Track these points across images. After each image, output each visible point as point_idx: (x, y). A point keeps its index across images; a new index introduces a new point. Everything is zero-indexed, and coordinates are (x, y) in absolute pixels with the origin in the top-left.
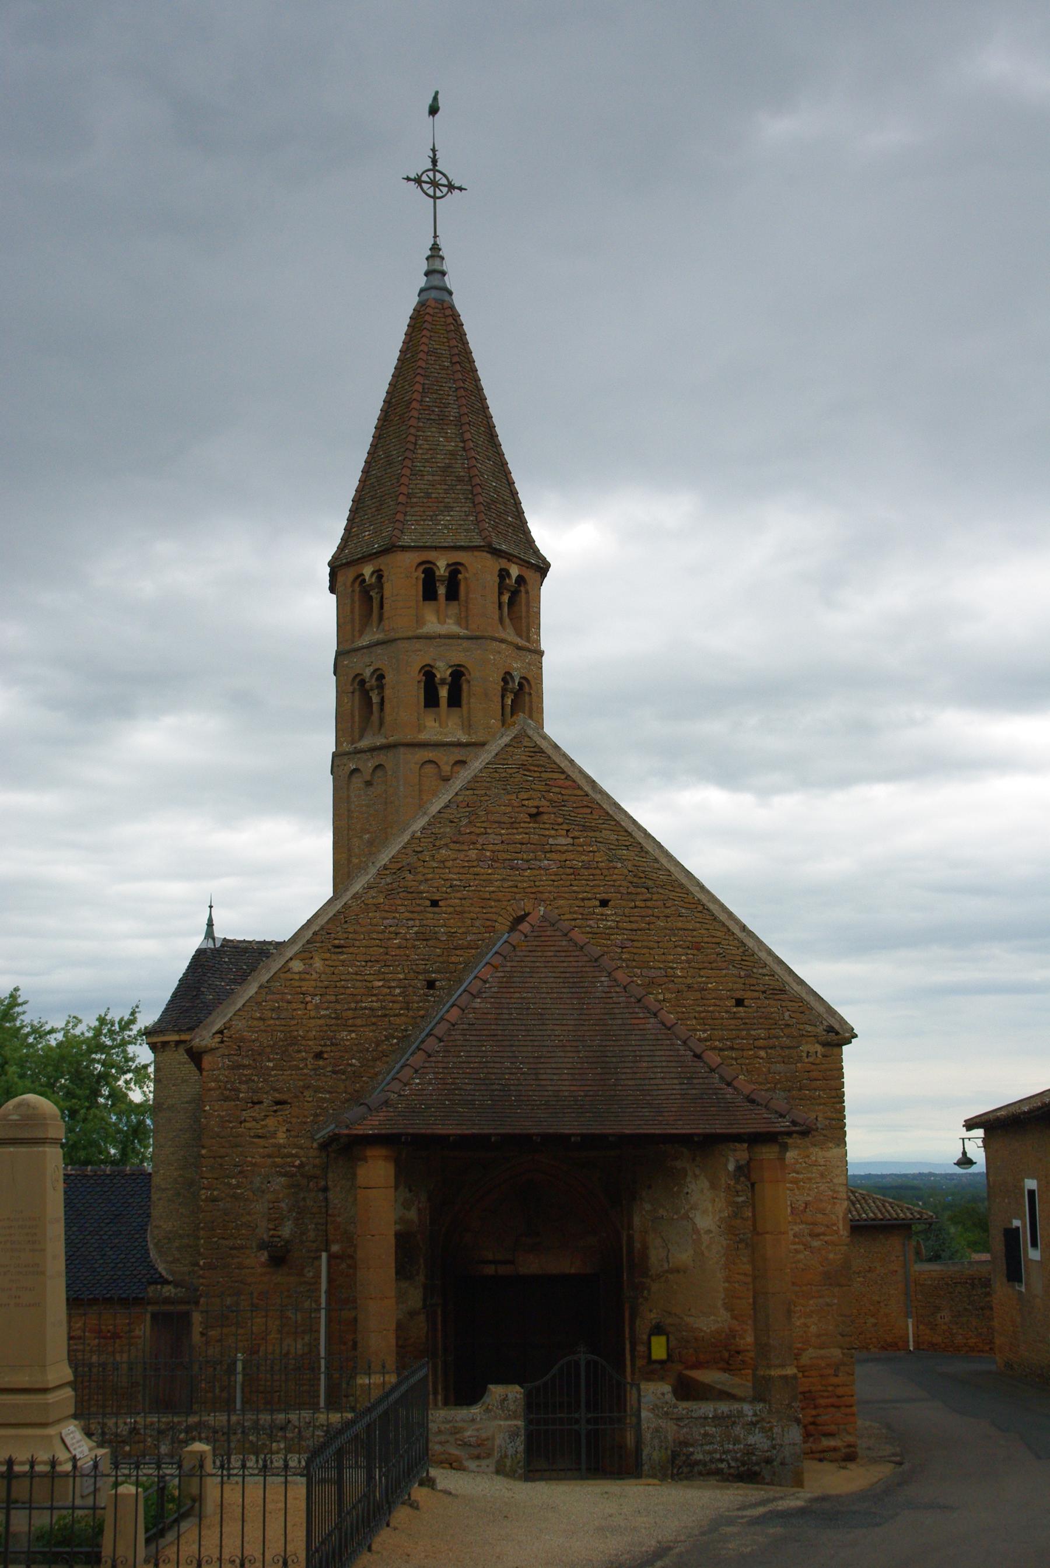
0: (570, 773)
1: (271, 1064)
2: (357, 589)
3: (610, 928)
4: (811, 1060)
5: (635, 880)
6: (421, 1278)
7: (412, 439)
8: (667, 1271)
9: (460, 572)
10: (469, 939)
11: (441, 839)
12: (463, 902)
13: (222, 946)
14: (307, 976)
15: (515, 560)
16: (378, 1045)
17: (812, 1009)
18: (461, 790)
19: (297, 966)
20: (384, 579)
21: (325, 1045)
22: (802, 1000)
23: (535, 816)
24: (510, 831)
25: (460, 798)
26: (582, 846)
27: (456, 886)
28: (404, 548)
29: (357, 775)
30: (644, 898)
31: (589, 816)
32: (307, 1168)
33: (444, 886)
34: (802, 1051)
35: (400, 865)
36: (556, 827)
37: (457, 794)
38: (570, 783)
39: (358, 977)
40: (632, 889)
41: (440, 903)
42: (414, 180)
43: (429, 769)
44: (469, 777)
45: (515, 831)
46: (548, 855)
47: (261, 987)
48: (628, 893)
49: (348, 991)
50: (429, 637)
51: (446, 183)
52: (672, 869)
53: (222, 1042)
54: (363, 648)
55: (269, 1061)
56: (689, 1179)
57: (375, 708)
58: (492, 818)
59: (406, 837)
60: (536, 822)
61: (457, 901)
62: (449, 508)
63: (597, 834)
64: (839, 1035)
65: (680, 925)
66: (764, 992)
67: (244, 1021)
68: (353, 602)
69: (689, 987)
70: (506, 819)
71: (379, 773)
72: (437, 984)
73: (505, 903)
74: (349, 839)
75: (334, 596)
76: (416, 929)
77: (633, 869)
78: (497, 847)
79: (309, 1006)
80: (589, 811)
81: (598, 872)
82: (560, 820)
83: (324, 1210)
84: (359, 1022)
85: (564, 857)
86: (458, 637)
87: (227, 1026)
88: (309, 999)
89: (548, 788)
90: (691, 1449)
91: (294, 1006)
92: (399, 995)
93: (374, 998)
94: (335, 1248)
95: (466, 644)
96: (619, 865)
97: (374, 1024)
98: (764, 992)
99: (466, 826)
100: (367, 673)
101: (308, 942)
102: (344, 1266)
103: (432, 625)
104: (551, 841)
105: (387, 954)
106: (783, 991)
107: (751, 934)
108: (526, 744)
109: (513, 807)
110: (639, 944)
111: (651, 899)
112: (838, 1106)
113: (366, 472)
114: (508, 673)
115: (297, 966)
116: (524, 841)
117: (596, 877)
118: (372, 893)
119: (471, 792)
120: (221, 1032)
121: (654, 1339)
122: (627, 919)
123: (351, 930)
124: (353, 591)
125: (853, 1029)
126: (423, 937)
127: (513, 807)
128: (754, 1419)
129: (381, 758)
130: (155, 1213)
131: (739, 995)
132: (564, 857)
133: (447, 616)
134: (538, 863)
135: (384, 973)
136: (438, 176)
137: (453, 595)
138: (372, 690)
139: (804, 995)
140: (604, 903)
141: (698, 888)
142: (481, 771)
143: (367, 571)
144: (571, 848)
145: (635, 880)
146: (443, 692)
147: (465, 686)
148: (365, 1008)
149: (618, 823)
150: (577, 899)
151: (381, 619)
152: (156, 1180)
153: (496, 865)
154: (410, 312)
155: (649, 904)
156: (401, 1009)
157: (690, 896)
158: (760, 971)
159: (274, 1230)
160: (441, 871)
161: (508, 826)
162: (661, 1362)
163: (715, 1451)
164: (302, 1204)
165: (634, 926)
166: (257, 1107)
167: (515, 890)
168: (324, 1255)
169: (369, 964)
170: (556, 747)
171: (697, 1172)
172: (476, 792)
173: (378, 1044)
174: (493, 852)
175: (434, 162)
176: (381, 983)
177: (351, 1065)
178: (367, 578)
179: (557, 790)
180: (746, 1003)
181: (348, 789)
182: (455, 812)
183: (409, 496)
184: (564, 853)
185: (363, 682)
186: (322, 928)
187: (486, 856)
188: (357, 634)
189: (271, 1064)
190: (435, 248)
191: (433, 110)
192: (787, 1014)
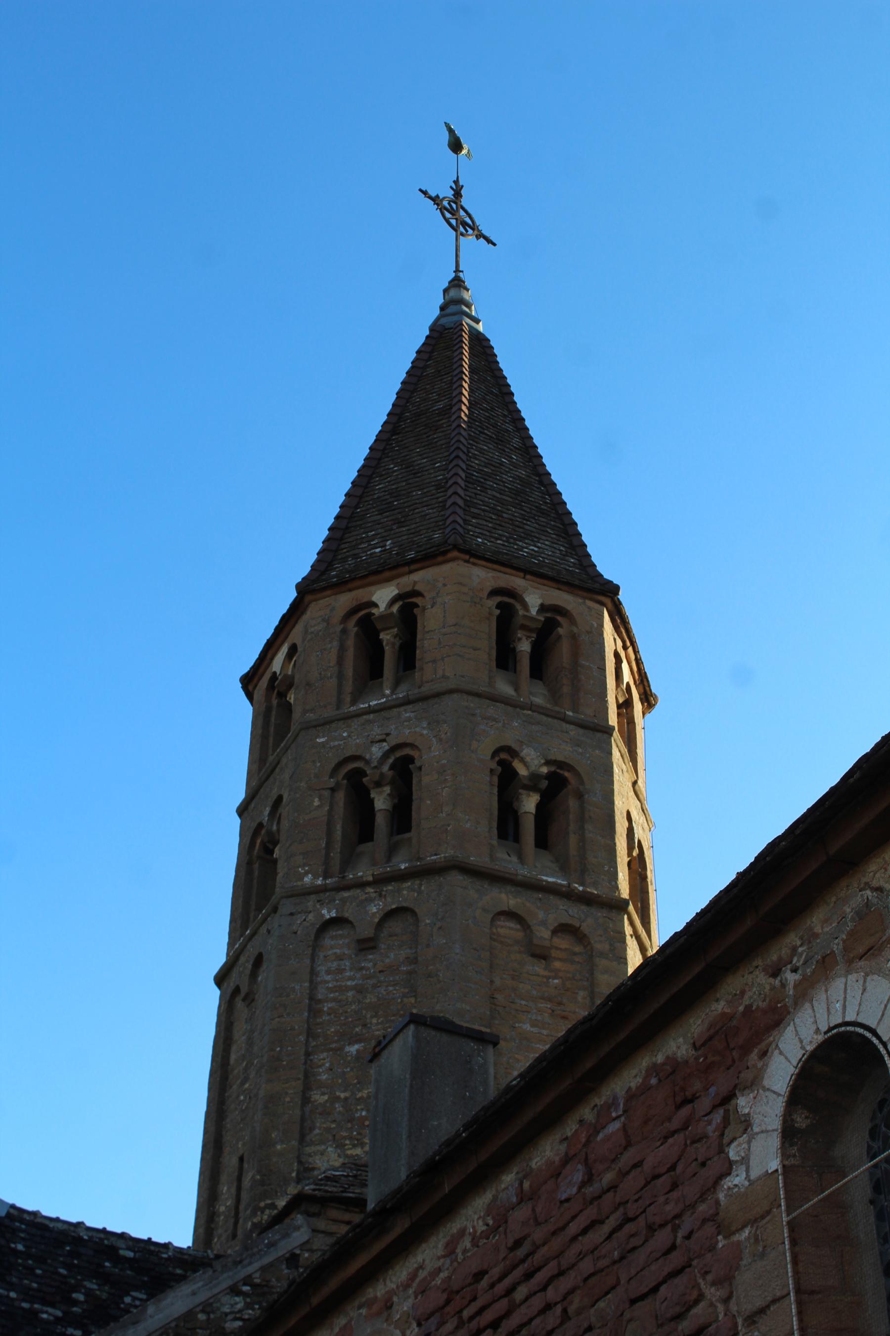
2: (352, 626)
9: (559, 625)
13: (8, 1215)
28: (473, 555)
43: (508, 929)
54: (370, 711)
68: (342, 649)
71: (396, 926)
74: (308, 1054)
95: (573, 731)
100: (377, 751)
124: (344, 631)
129: (406, 894)
138: (378, 784)
143: (383, 596)
147: (573, 803)
191: (456, 146)
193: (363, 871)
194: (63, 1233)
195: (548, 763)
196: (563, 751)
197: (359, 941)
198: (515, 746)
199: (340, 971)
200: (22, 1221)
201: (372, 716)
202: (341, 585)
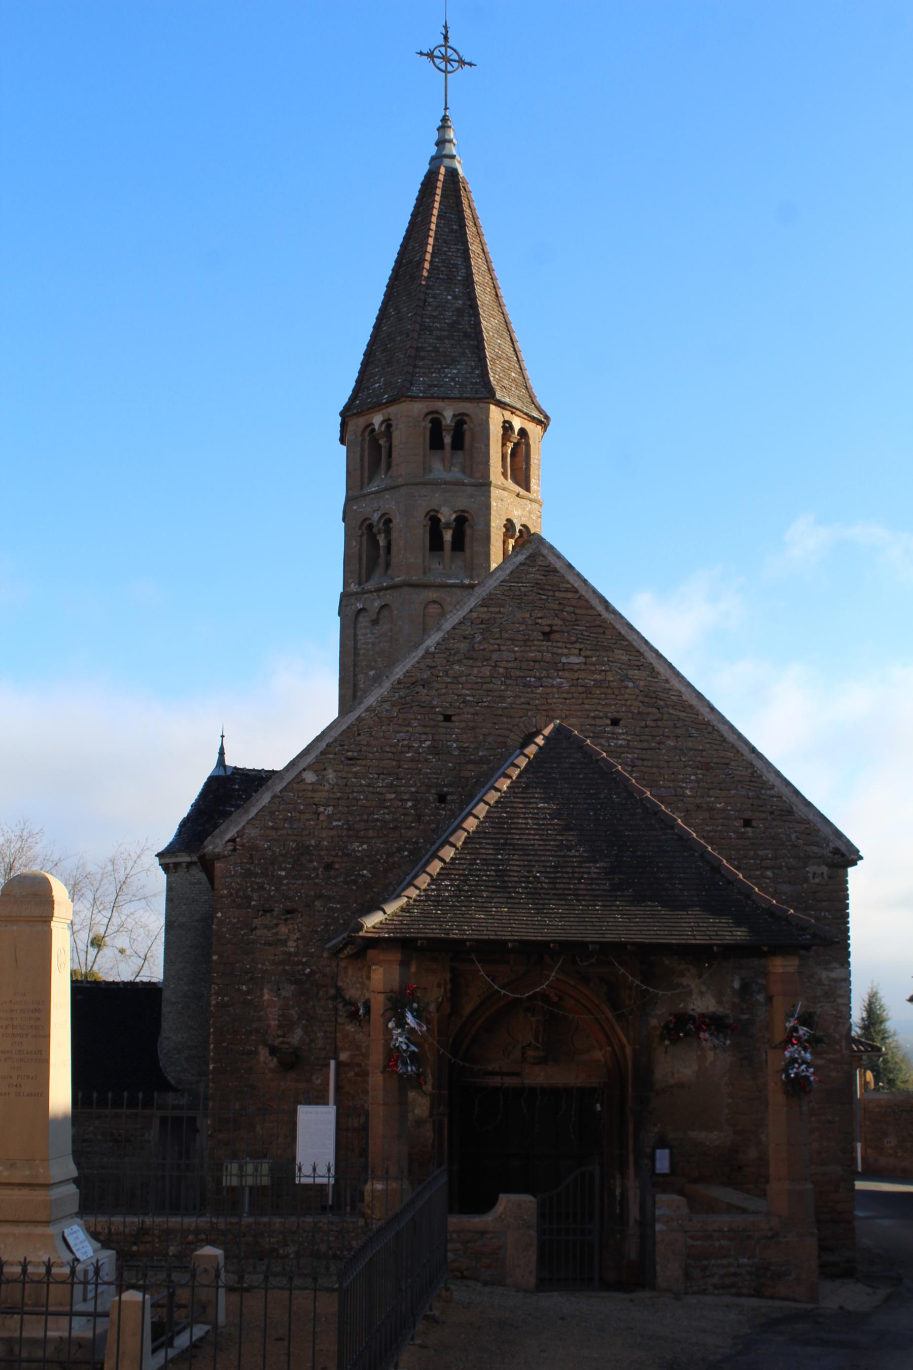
0: (583, 593)
1: (283, 873)
3: (621, 746)
4: (817, 880)
5: (646, 700)
7: (422, 296)
9: (465, 423)
10: (481, 754)
11: (455, 654)
12: (476, 717)
13: (233, 773)
14: (320, 788)
15: (518, 413)
16: (390, 855)
17: (818, 831)
18: (475, 607)
19: (310, 777)
20: (393, 428)
21: (337, 856)
22: (808, 822)
23: (547, 635)
24: (523, 648)
25: (475, 615)
26: (594, 665)
27: (469, 701)
29: (363, 614)
30: (656, 718)
31: (602, 636)
32: (317, 976)
33: (457, 701)
34: (808, 872)
35: (414, 679)
36: (569, 646)
37: (471, 611)
39: (371, 789)
40: (643, 709)
41: (453, 718)
42: (427, 55)
44: (484, 594)
45: (528, 649)
46: (560, 673)
47: (273, 797)
48: (639, 713)
49: (360, 803)
50: (435, 484)
51: (457, 59)
52: (683, 689)
53: (235, 850)
54: (372, 493)
55: (281, 870)
56: (694, 996)
57: (382, 552)
59: (420, 652)
60: (548, 640)
61: (469, 716)
62: (454, 362)
63: (610, 654)
64: (847, 856)
65: (690, 745)
66: (772, 813)
67: (257, 831)
68: (362, 450)
69: (698, 807)
70: (520, 637)
71: (385, 612)
72: (449, 797)
73: (517, 720)
74: (355, 675)
75: (344, 448)
76: (428, 743)
78: (510, 665)
79: (322, 818)
80: (601, 630)
81: (610, 691)
82: (573, 639)
83: (333, 1019)
84: (371, 833)
85: (576, 675)
86: (459, 484)
87: (240, 834)
88: (322, 809)
89: (562, 607)
90: (706, 1263)
91: (307, 816)
92: (411, 807)
93: (386, 811)
94: (343, 1056)
95: (469, 490)
96: (631, 685)
97: (385, 836)
98: (772, 813)
99: (480, 642)
100: (376, 517)
101: (322, 753)
102: (352, 1074)
103: (439, 471)
104: (564, 660)
105: (399, 767)
106: (790, 812)
107: (760, 756)
108: (540, 563)
110: (649, 763)
111: (661, 720)
112: (843, 927)
113: (377, 327)
114: (509, 521)
115: (310, 777)
116: (539, 657)
117: (608, 696)
118: (386, 706)
119: (485, 609)
120: (233, 840)
121: (658, 1152)
122: (638, 738)
123: (364, 742)
125: (858, 851)
126: (435, 750)
127: (526, 625)
128: (770, 1234)
129: (388, 597)
130: (165, 1025)
131: (748, 815)
132: (576, 675)
133: (452, 465)
134: (550, 681)
135: (396, 786)
136: (450, 51)
137: (458, 444)
138: (379, 533)
139: (811, 817)
140: (615, 722)
141: (708, 710)
142: (495, 589)
143: (377, 420)
144: (583, 667)
145: (646, 700)
146: (448, 536)
148: (378, 820)
149: (631, 645)
150: (588, 717)
151: (389, 466)
152: (166, 994)
153: (508, 682)
154: (421, 179)
155: (660, 723)
156: (412, 822)
158: (769, 792)
159: (284, 1036)
160: (453, 686)
161: (522, 643)
162: (663, 1175)
165: (645, 745)
166: (268, 915)
167: (527, 707)
168: (332, 1063)
169: (382, 776)
170: (570, 566)
171: (704, 989)
172: (491, 609)
173: (390, 855)
174: (506, 668)
175: (446, 38)
176: (393, 796)
177: (363, 876)
178: (377, 427)
179: (571, 609)
180: (754, 823)
181: (355, 628)
182: (469, 629)
183: (418, 349)
184: (576, 671)
185: (370, 526)
186: (335, 740)
187: (499, 673)
188: (366, 481)
189: (283, 873)
190: (445, 119)
192: (793, 836)
193: (370, 586)
194: (255, 776)
195: (455, 512)
196: (463, 502)
197: (372, 621)
198: (436, 508)
199: (366, 634)
200: (238, 774)
201: (373, 496)
202: (358, 414)
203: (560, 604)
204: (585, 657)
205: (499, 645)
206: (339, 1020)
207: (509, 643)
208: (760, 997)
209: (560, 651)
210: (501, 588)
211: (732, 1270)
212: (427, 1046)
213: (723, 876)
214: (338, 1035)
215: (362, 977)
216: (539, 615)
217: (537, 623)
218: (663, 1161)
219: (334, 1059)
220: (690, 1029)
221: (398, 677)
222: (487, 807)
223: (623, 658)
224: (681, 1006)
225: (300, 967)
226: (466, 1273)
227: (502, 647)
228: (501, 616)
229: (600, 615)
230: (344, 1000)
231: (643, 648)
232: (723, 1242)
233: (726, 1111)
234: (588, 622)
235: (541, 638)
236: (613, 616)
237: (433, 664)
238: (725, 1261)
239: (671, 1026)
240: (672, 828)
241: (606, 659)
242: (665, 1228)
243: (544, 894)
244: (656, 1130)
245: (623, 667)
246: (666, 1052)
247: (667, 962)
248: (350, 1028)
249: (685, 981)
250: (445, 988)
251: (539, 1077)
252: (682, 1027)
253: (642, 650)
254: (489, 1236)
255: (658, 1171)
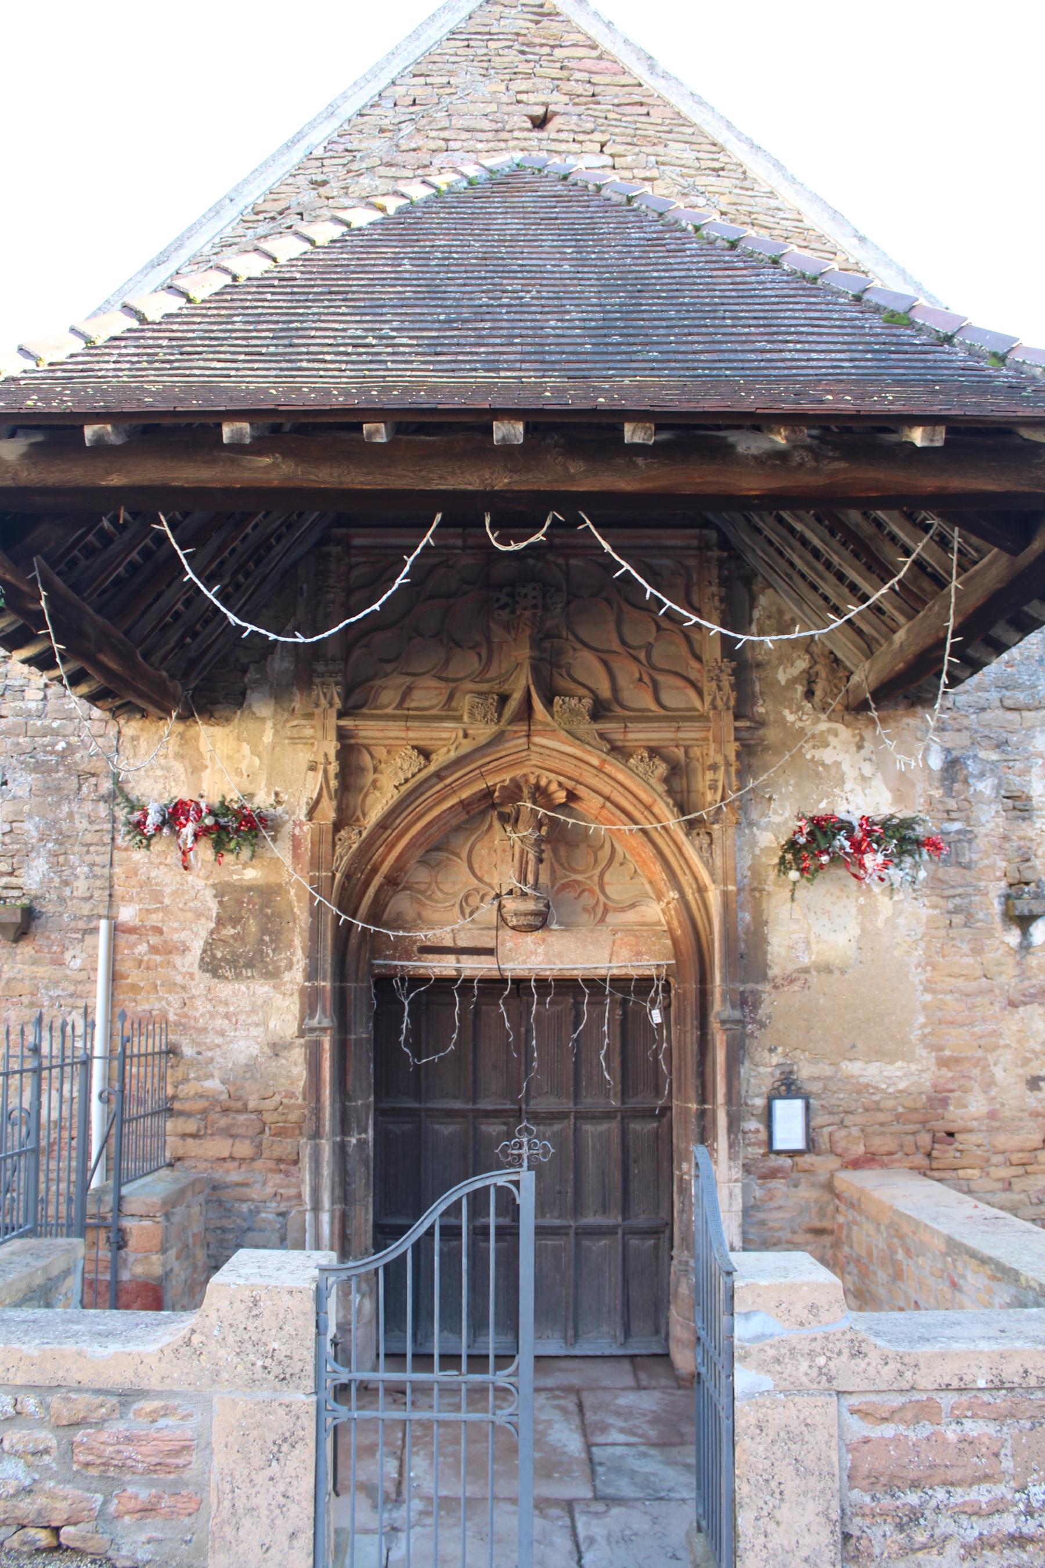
6: (296, 976)
8: (806, 970)
11: (362, 159)
23: (540, 123)
24: (492, 145)
25: (400, 90)
31: (644, 119)
32: (78, 756)
36: (580, 137)
38: (608, 64)
44: (418, 53)
45: (502, 145)
52: (804, 206)
56: (848, 786)
58: (457, 122)
63: (660, 149)
70: (486, 124)
77: (731, 209)
80: (643, 110)
82: (589, 126)
83: (107, 839)
89: (565, 74)
90: (913, 1498)
94: (127, 914)
96: (701, 201)
99: (410, 136)
102: (143, 948)
109: (499, 104)
119: (421, 80)
121: (779, 1105)
127: (499, 104)
141: (855, 241)
157: (840, 257)
159: (11, 874)
162: (792, 1154)
163: (998, 1508)
164: (65, 826)
171: (867, 769)
172: (429, 80)
179: (585, 76)
182: (391, 113)
203: (561, 68)
204: (612, 156)
205: (447, 140)
206: (119, 841)
207: (465, 135)
208: (985, 787)
209: (563, 147)
210: (452, 43)
211: (1008, 1523)
212: (292, 892)
213: (921, 330)
214: (117, 870)
215: (166, 756)
216: (523, 88)
217: (519, 102)
218: (789, 1125)
219: (108, 917)
220: (842, 848)
221: (251, 199)
222: (307, 247)
223: (685, 155)
224: (823, 805)
225: (47, 739)
226: (68, 1534)
227: (452, 145)
228: (448, 91)
229: (640, 85)
230: (128, 800)
231: (723, 137)
232: (973, 1428)
233: (922, 1020)
234: (617, 96)
235: (529, 125)
236: (663, 82)
237: (320, 178)
238: (981, 1495)
239: (802, 840)
240: (775, 262)
241: (653, 159)
242: (767, 1382)
243: (393, 362)
244: (775, 1060)
245: (685, 171)
246: (793, 899)
247: (791, 718)
248: (139, 856)
249: (828, 755)
250: (325, 772)
251: (531, 957)
252: (820, 845)
253: (720, 140)
254: (149, 1405)
255: (778, 1145)
